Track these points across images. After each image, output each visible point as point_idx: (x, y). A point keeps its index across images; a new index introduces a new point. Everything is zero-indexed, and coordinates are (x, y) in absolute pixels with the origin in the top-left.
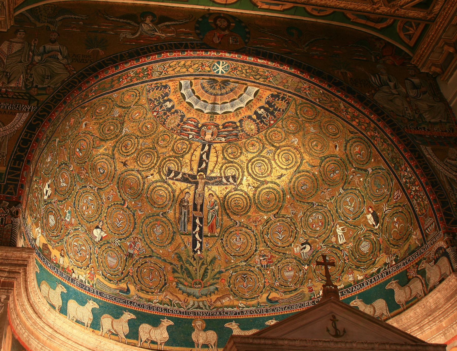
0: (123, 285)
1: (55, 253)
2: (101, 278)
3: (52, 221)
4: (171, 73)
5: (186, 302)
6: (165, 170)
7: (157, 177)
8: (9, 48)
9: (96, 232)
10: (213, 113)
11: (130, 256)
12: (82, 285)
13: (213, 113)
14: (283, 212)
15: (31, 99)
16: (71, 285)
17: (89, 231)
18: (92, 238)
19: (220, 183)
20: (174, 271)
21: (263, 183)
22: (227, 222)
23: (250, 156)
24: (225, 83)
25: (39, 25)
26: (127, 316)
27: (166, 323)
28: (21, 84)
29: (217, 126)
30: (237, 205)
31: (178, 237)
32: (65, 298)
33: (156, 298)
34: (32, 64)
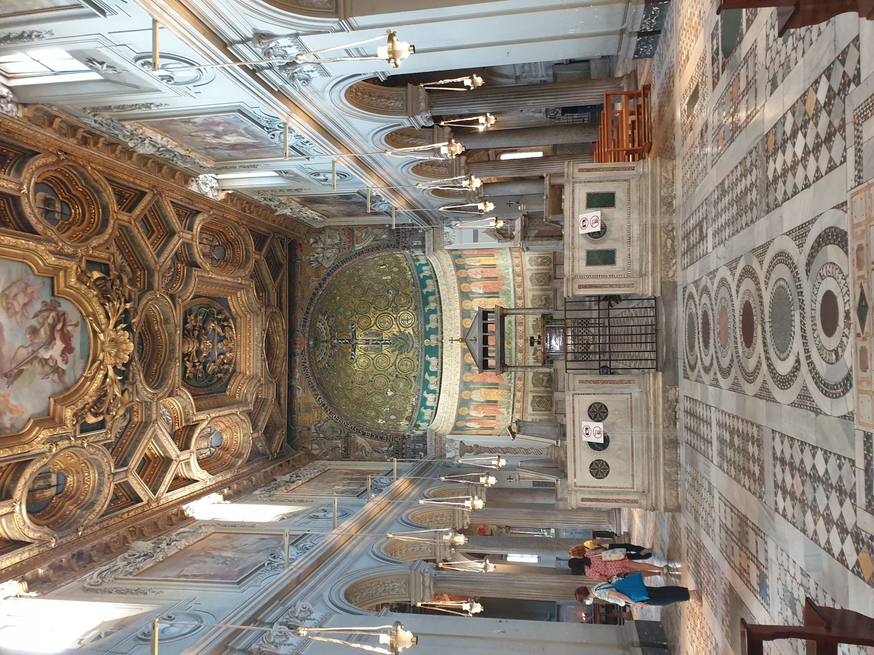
0: (412, 379)
1: (407, 414)
2: (411, 390)
3: (393, 417)
4: (316, 368)
5: (416, 348)
6: (351, 361)
7: (355, 365)
8: (316, 449)
9: (390, 394)
10: (326, 341)
11: (397, 375)
12: (418, 399)
13: (326, 341)
14: (371, 301)
15: (348, 436)
16: (419, 405)
17: (391, 398)
18: (393, 396)
19: (355, 331)
20: (401, 353)
21: (355, 311)
22: (375, 328)
23: (343, 318)
24: (316, 339)
25: (298, 437)
26: (427, 376)
27: (428, 358)
28: (339, 441)
29: (331, 338)
30: (366, 322)
31: (384, 352)
32: (426, 407)
33: (416, 363)
34: (325, 437)
